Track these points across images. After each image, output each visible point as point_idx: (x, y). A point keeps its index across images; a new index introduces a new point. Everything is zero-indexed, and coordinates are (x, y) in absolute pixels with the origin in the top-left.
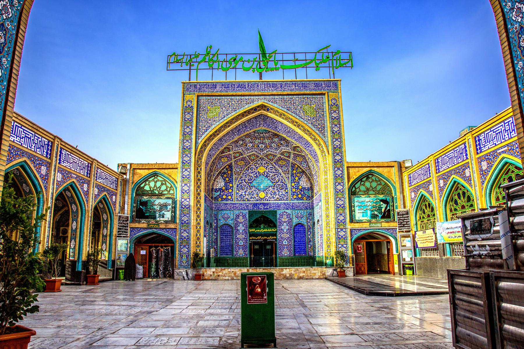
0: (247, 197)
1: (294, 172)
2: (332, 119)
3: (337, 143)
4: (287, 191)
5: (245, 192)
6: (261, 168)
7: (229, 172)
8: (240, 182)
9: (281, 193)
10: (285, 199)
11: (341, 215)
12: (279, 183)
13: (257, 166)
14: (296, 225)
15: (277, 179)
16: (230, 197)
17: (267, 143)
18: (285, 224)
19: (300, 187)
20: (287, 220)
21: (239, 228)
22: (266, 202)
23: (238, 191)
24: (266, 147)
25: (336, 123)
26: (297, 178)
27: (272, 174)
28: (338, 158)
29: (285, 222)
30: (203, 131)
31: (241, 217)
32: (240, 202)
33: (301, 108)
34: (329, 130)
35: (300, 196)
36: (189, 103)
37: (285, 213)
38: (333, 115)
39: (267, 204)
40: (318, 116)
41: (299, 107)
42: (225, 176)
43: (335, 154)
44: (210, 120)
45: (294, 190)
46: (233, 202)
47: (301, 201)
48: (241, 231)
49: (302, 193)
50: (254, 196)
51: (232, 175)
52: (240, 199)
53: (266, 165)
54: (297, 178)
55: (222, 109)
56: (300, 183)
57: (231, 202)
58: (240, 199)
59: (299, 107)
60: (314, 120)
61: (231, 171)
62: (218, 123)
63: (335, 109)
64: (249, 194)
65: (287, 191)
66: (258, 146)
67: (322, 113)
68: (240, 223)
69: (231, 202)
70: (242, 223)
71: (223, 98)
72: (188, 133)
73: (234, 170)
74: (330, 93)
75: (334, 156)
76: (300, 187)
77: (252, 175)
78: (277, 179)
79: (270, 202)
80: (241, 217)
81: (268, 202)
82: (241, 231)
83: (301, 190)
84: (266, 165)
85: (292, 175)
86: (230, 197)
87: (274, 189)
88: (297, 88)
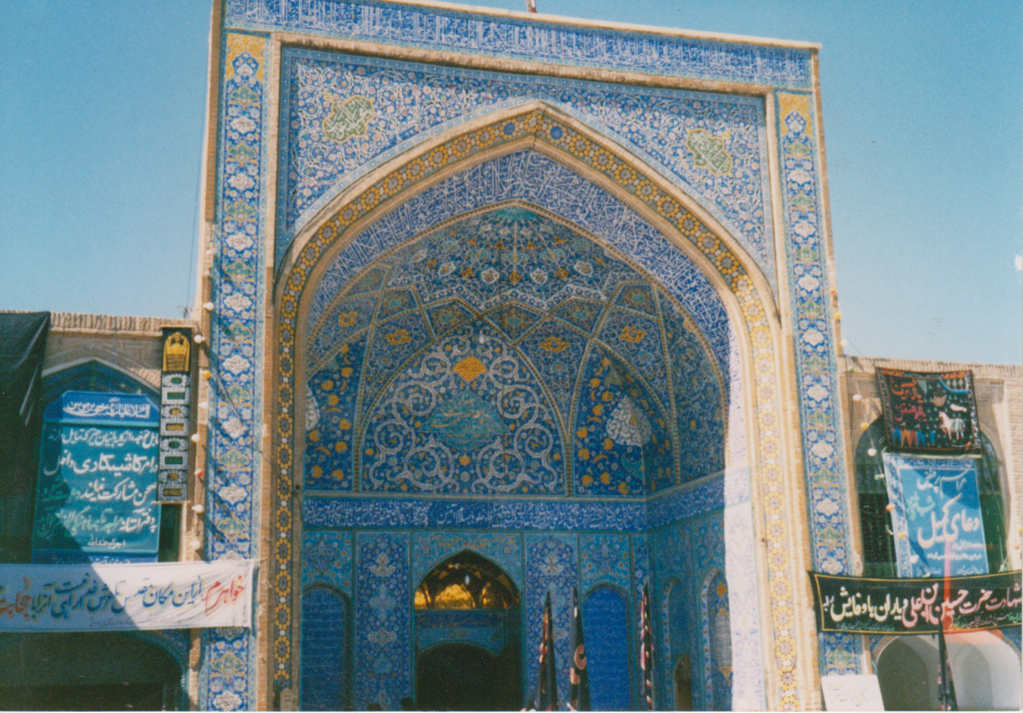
0: (407, 474)
1: (595, 383)
2: (791, 190)
3: (809, 283)
4: (556, 457)
5: (399, 455)
6: (470, 361)
7: (347, 372)
8: (382, 412)
9: (535, 465)
10: (551, 485)
11: (832, 554)
12: (530, 425)
13: (456, 351)
14: (592, 593)
15: (524, 407)
16: (338, 475)
17: (515, 263)
18: (552, 586)
19: (607, 445)
20: (561, 568)
21: (373, 602)
22: (482, 497)
23: (369, 452)
24: (505, 281)
25: (804, 207)
26: (598, 410)
27: (508, 389)
28: (813, 337)
29: (551, 579)
30: (307, 192)
31: (382, 558)
32: (380, 495)
33: (679, 139)
34: (779, 228)
35: (606, 478)
36: (244, 69)
37: (551, 545)
38: (793, 175)
39: (487, 506)
40: (739, 174)
41: (672, 136)
42: (328, 385)
43: (804, 323)
44: (335, 151)
45: (584, 454)
46: (352, 494)
47: (612, 499)
48: (383, 617)
49: (615, 466)
50: (433, 473)
51: (354, 380)
52: (377, 483)
53: (489, 353)
54: (598, 410)
55: (384, 110)
56: (611, 426)
57: (344, 494)
58: (377, 483)
59: (672, 136)
60: (726, 191)
61: (355, 366)
62: (366, 169)
63: (799, 155)
64: (416, 463)
65: (556, 457)
66: (478, 276)
67: (755, 166)
68: (380, 581)
69: (344, 494)
70: (386, 580)
71: (387, 64)
72: (241, 194)
73: (366, 364)
74: (782, 96)
75: (801, 331)
76: (607, 445)
77: (430, 387)
78: (524, 407)
79: (498, 497)
80: (382, 558)
81: (489, 497)
82: (383, 617)
83: (611, 457)
84: (489, 353)
85: (586, 392)
86: (338, 475)
87: (510, 447)
88: (666, 60)
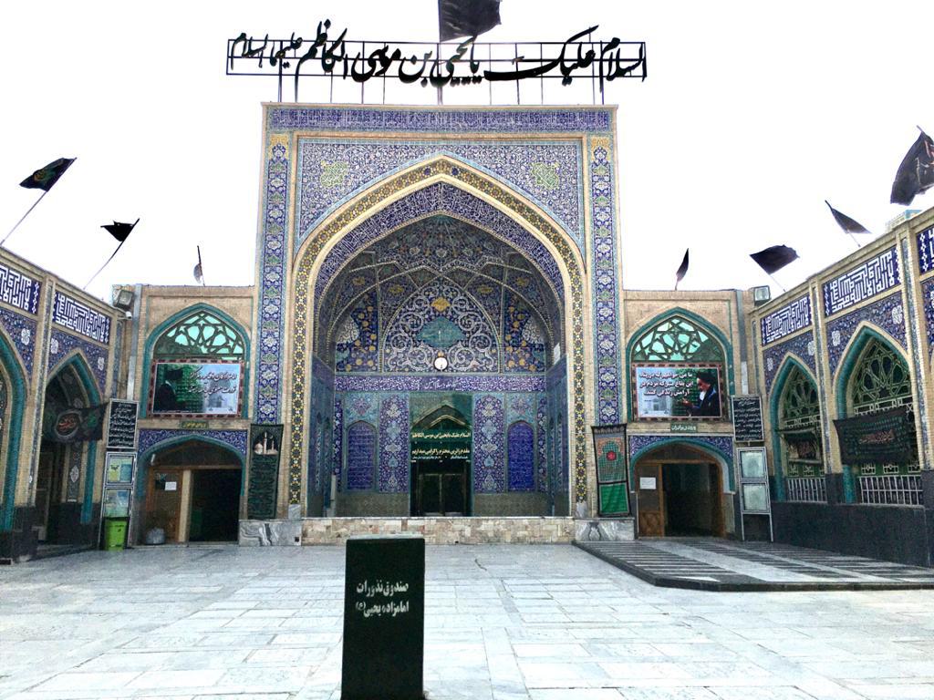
0: (408, 362)
1: (512, 309)
4: (494, 351)
5: (406, 351)
7: (370, 309)
8: (394, 330)
9: (481, 356)
10: (490, 367)
11: (609, 404)
15: (474, 324)
16: (370, 363)
20: (494, 412)
23: (388, 351)
24: (450, 256)
25: (603, 204)
26: (516, 324)
27: (462, 315)
28: (605, 280)
30: (311, 216)
31: (394, 407)
32: (394, 374)
33: (527, 169)
34: (588, 218)
35: (522, 362)
38: (597, 186)
42: (361, 316)
44: (326, 193)
50: (423, 361)
51: (375, 314)
53: (450, 295)
54: (516, 324)
55: (354, 168)
58: (392, 368)
60: (555, 197)
61: (374, 305)
66: (434, 252)
68: (392, 419)
72: (276, 220)
73: (380, 304)
75: (597, 277)
78: (474, 324)
80: (394, 407)
84: (450, 295)
86: (370, 363)
88: (519, 123)
